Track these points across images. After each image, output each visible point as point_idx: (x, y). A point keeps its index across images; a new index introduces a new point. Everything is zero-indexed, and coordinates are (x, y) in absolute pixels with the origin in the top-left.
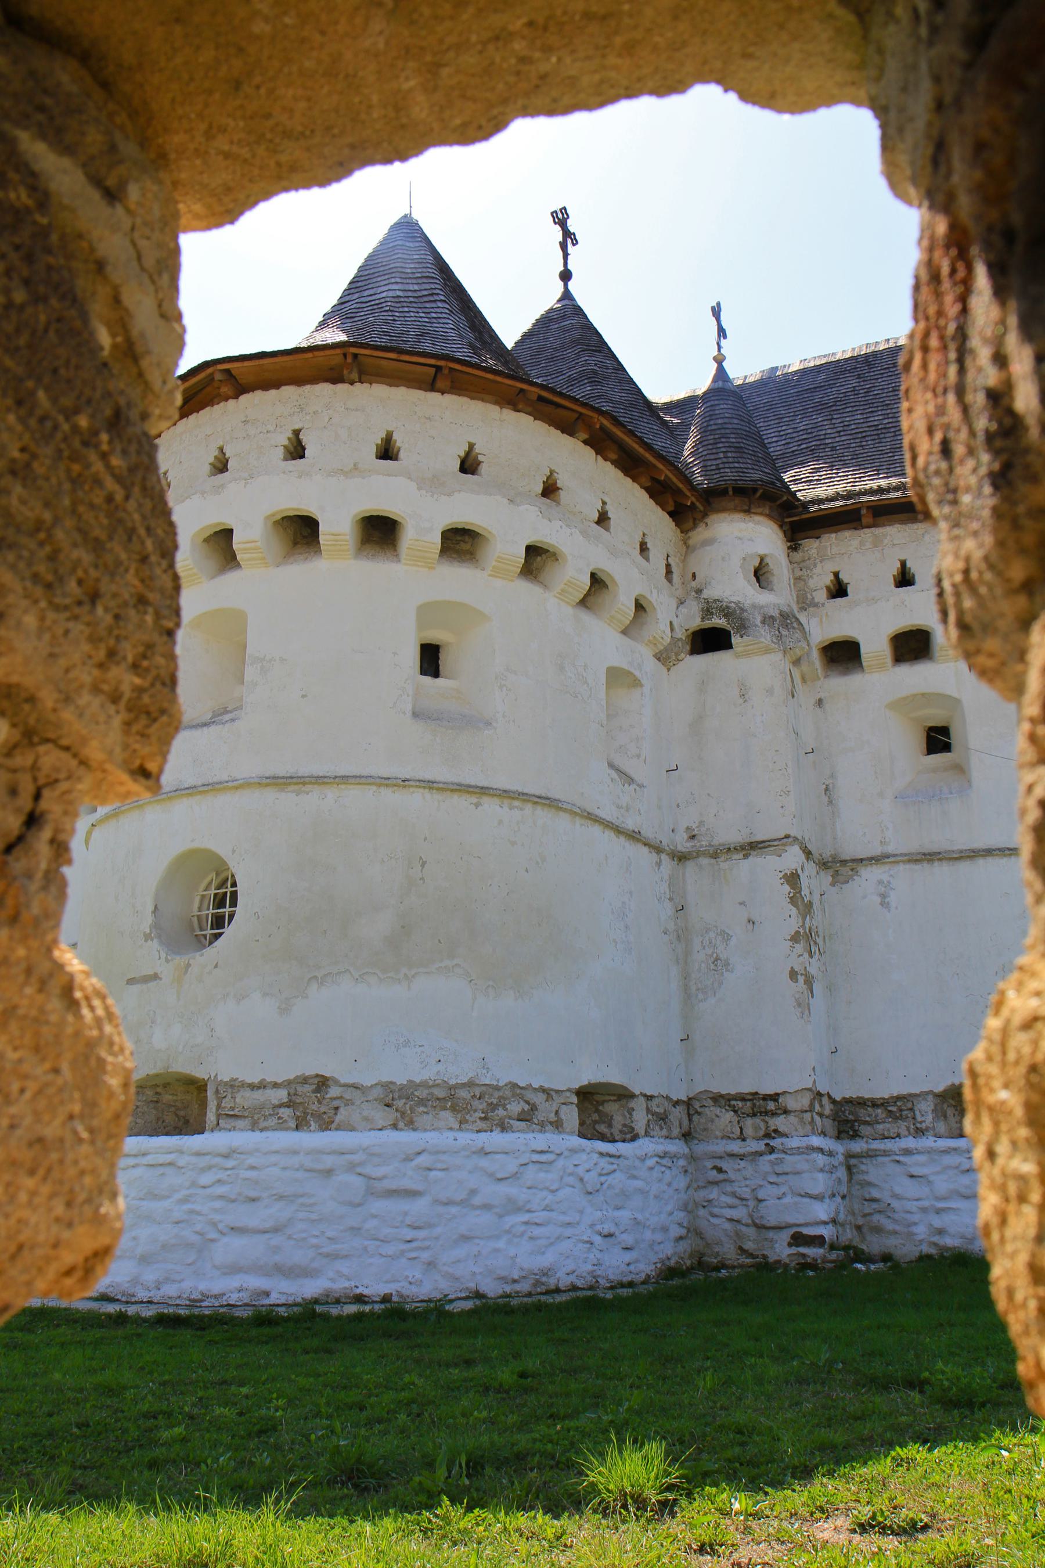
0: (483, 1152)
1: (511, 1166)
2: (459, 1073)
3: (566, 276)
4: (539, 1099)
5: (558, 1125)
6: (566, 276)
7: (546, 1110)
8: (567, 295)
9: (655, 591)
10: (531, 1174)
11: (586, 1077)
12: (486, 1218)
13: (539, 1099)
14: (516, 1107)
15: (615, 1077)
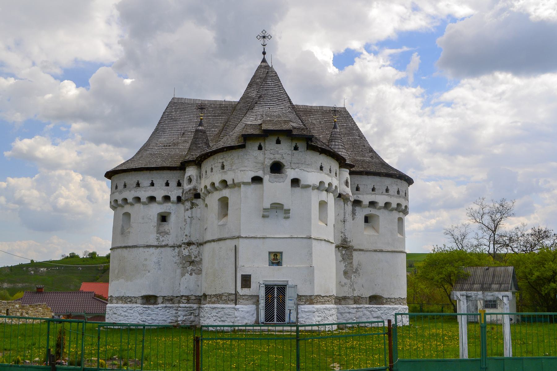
0: (122, 307)
1: (125, 309)
2: (122, 295)
3: (264, 53)
4: (133, 299)
5: (136, 303)
6: (264, 53)
7: (134, 300)
8: (264, 61)
9: (170, 193)
10: (129, 311)
11: (144, 293)
12: (122, 317)
13: (133, 299)
14: (129, 300)
15: (151, 293)
